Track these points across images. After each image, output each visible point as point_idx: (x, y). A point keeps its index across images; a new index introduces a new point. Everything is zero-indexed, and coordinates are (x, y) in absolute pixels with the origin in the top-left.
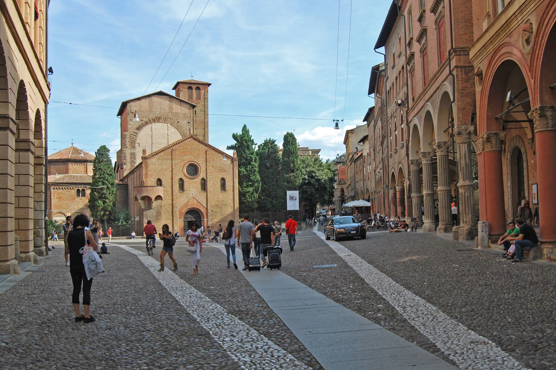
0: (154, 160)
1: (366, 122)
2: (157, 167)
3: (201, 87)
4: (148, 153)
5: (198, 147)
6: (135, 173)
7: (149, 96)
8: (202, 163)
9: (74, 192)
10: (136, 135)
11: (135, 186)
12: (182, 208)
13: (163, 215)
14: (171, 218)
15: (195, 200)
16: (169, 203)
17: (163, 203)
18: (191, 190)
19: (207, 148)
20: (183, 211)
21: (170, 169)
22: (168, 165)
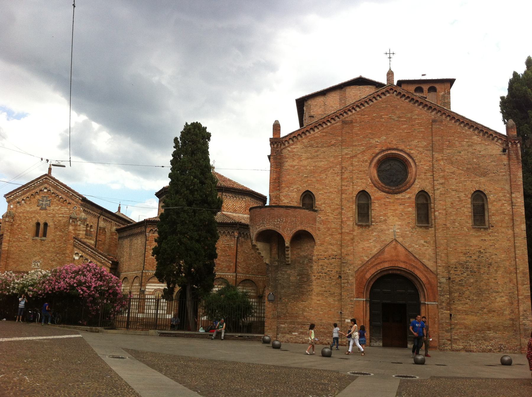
0: (297, 147)
2: (305, 163)
3: (437, 86)
4: (283, 133)
5: (409, 115)
13: (314, 283)
14: (337, 291)
15: (400, 248)
16: (330, 252)
17: (315, 253)
18: (388, 222)
19: (433, 115)
20: (368, 276)
21: (337, 169)
22: (332, 159)
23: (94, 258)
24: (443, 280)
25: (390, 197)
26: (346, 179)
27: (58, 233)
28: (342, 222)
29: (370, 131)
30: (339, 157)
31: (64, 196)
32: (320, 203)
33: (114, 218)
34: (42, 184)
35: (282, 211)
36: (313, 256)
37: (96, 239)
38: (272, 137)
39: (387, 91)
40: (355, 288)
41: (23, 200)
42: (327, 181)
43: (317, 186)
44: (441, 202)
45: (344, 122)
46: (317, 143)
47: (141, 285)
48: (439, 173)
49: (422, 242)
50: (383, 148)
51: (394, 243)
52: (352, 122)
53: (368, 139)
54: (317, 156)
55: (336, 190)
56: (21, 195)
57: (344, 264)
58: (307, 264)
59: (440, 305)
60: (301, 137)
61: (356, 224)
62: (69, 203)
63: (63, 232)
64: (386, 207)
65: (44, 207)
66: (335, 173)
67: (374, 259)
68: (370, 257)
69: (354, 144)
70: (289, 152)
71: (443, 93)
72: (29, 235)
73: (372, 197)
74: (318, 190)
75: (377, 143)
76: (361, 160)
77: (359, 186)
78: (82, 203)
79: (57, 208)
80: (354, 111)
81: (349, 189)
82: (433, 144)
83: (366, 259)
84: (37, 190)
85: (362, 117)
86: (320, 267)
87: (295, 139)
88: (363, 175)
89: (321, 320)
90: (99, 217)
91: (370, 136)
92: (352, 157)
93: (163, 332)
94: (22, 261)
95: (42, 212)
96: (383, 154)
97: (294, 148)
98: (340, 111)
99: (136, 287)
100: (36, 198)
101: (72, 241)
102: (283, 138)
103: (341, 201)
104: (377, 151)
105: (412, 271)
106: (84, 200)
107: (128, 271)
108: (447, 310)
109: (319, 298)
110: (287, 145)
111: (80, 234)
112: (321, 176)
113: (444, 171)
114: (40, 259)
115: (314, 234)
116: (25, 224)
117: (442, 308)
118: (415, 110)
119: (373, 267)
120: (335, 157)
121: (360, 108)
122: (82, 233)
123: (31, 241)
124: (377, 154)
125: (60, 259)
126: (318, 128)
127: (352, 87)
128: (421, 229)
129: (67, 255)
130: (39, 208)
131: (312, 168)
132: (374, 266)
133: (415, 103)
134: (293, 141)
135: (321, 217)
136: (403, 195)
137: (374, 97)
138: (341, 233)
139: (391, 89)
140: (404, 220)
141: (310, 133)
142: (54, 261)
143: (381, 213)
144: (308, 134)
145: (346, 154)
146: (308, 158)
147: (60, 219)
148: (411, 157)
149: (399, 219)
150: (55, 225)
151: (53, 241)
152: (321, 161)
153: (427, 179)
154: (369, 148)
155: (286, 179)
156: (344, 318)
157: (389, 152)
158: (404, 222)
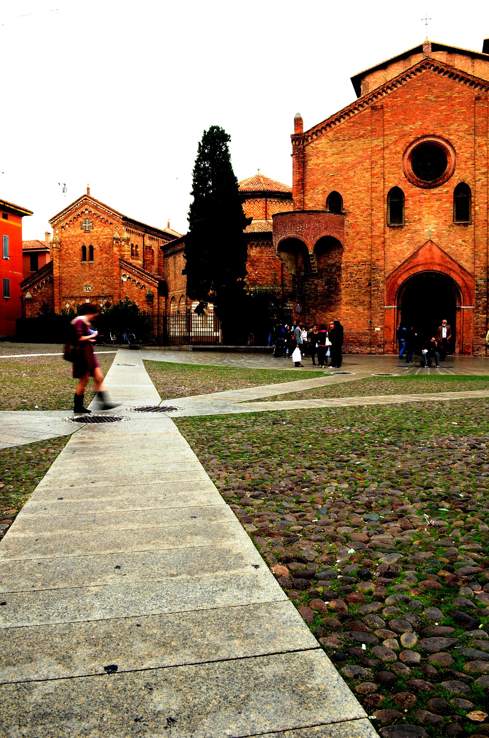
2: (330, 160)
4: (306, 128)
5: (448, 94)
8: (461, 138)
13: (343, 290)
14: (367, 299)
15: (435, 249)
16: (359, 258)
17: (344, 260)
18: (422, 221)
20: (400, 281)
21: (367, 164)
22: (360, 153)
23: (141, 279)
25: (425, 193)
26: (376, 175)
27: (105, 255)
28: (372, 224)
29: (403, 117)
30: (369, 150)
31: (105, 217)
32: (348, 204)
33: (161, 235)
34: (82, 205)
35: (304, 217)
36: (341, 263)
37: (144, 258)
38: (293, 133)
39: (423, 67)
40: (387, 295)
41: (67, 224)
43: (346, 186)
44: (482, 195)
45: (373, 108)
46: (344, 136)
47: (187, 304)
48: (481, 161)
49: (460, 241)
50: (419, 136)
51: (429, 244)
52: (382, 107)
53: (400, 126)
54: (344, 150)
55: (365, 188)
56: (65, 219)
57: (374, 271)
58: (335, 273)
59: (476, 309)
60: (326, 130)
61: (388, 226)
62: (111, 223)
63: (108, 254)
64: (421, 204)
65: (87, 229)
66: (365, 169)
67: (406, 263)
68: (403, 261)
69: (386, 133)
70: (313, 149)
72: (77, 260)
73: (406, 194)
74: (346, 190)
75: (412, 130)
76: (394, 151)
77: (391, 182)
78: (124, 222)
79: (100, 229)
80: (384, 94)
81: (379, 186)
82: (475, 126)
83: (399, 264)
84: (79, 212)
85: (395, 100)
86: (349, 275)
87: (319, 134)
88: (396, 169)
89: (351, 329)
90: (144, 235)
91: (403, 122)
92: (383, 149)
93: (196, 347)
94: (74, 287)
95: (86, 234)
96: (418, 143)
97: (318, 144)
98: (368, 96)
99: (183, 306)
100: (79, 221)
101: (118, 263)
102: (306, 132)
103: (371, 201)
104: (412, 140)
105: (448, 274)
106: (125, 218)
107: (175, 290)
108: (483, 314)
109: (349, 307)
110: (310, 141)
111: (124, 255)
112: (349, 174)
114: (90, 283)
115: (341, 240)
116: (72, 249)
117: (478, 312)
118: (456, 87)
119: (405, 272)
120: (363, 150)
121: (391, 89)
122: (127, 254)
123: (80, 265)
125: (109, 282)
126: (344, 118)
127: (418, 55)
128: (459, 227)
129: (115, 277)
130: (83, 231)
131: (339, 165)
132: (407, 270)
133: (455, 79)
134: (317, 135)
135: (349, 220)
136: (440, 189)
137: (408, 76)
138: (372, 237)
139: (428, 64)
140: (440, 217)
141: (335, 124)
142: (103, 284)
143: (416, 212)
144: (333, 126)
145: (377, 146)
146: (334, 154)
147: (104, 240)
148: (450, 144)
149: (436, 217)
150: (100, 247)
151: (100, 264)
152: (348, 156)
153: (468, 168)
154: (403, 136)
155: (310, 180)
156: (373, 327)
157: (425, 140)
158: (440, 220)
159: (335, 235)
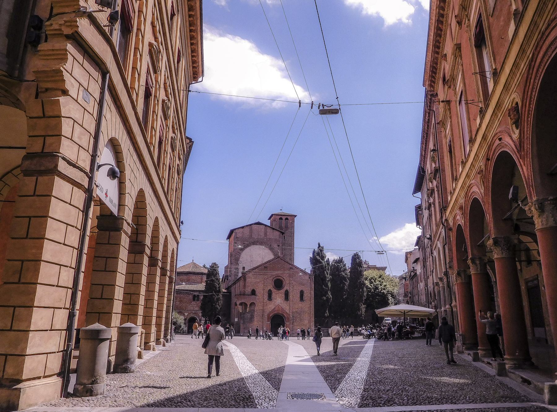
0: (250, 275)
1: (417, 247)
5: (284, 266)
6: (237, 284)
7: (251, 225)
9: (191, 297)
10: (239, 254)
11: (236, 294)
12: (270, 313)
17: (256, 309)
21: (263, 282)
24: (291, 316)
42: (259, 286)
52: (267, 267)
71: (291, 222)
113: (293, 284)
124: (274, 278)
135: (257, 297)
159: (254, 302)
